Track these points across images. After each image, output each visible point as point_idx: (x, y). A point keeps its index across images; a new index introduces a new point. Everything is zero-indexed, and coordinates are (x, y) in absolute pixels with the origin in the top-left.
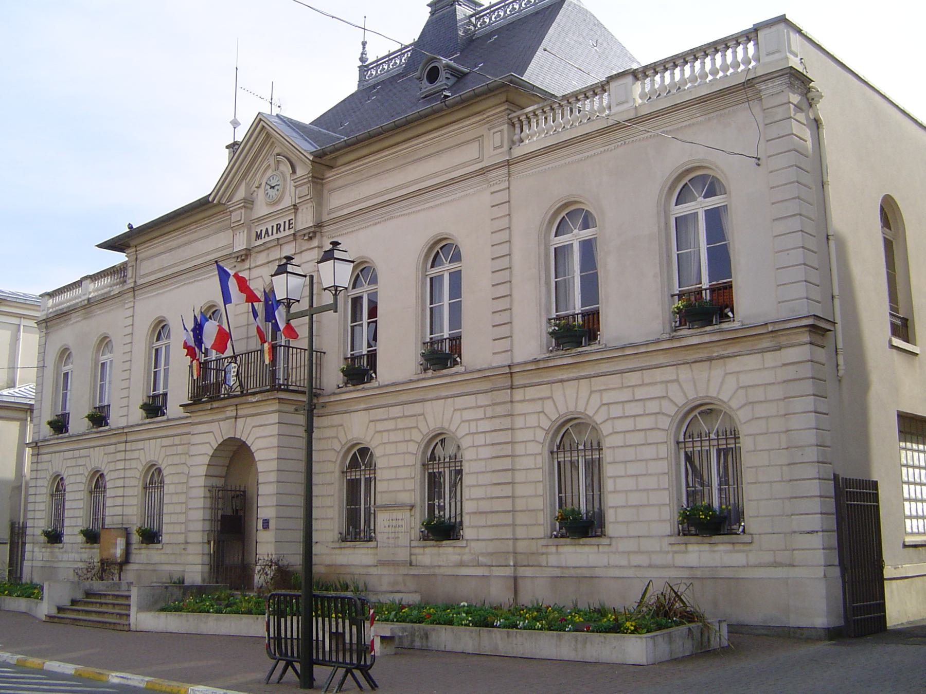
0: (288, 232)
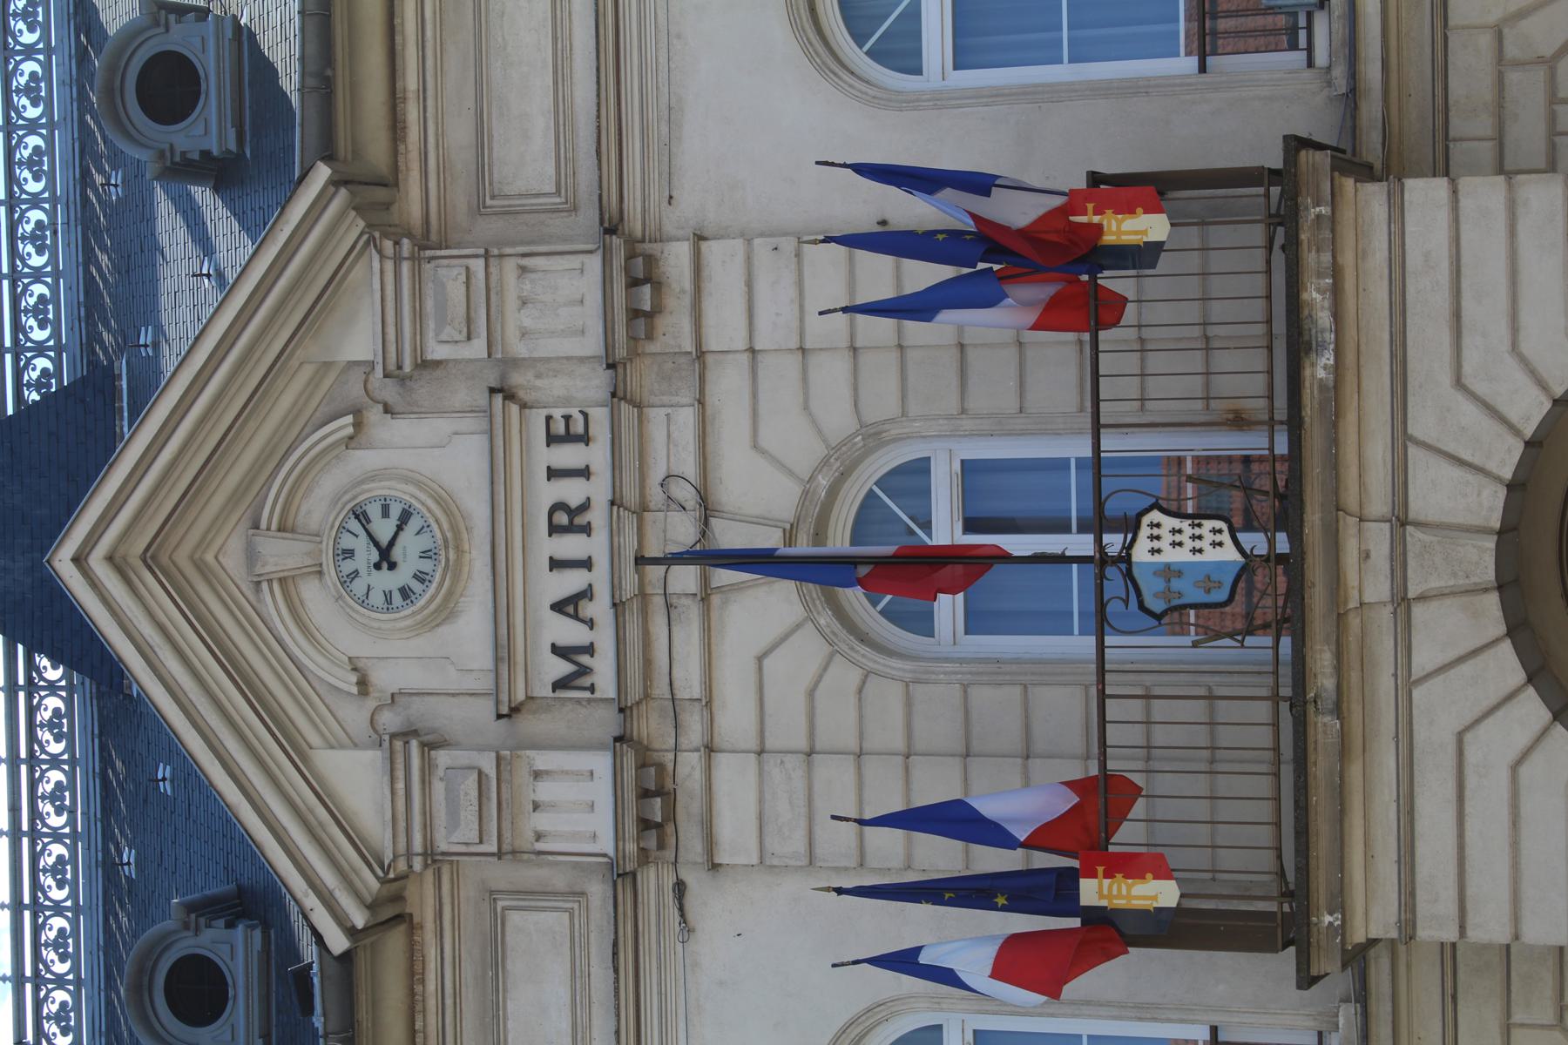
0: (596, 455)
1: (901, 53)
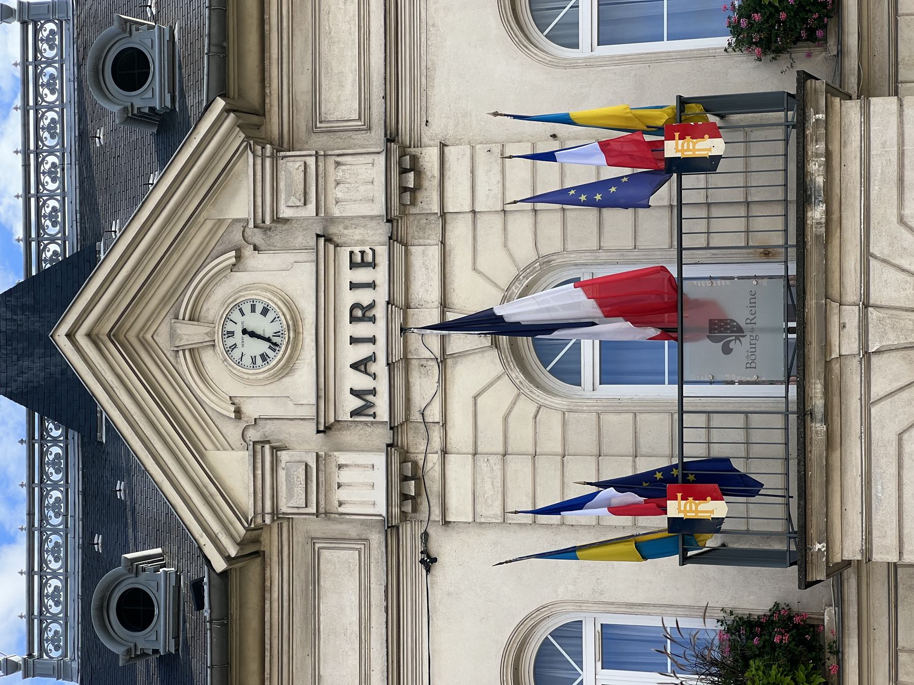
0: (380, 275)
1: (567, 36)
